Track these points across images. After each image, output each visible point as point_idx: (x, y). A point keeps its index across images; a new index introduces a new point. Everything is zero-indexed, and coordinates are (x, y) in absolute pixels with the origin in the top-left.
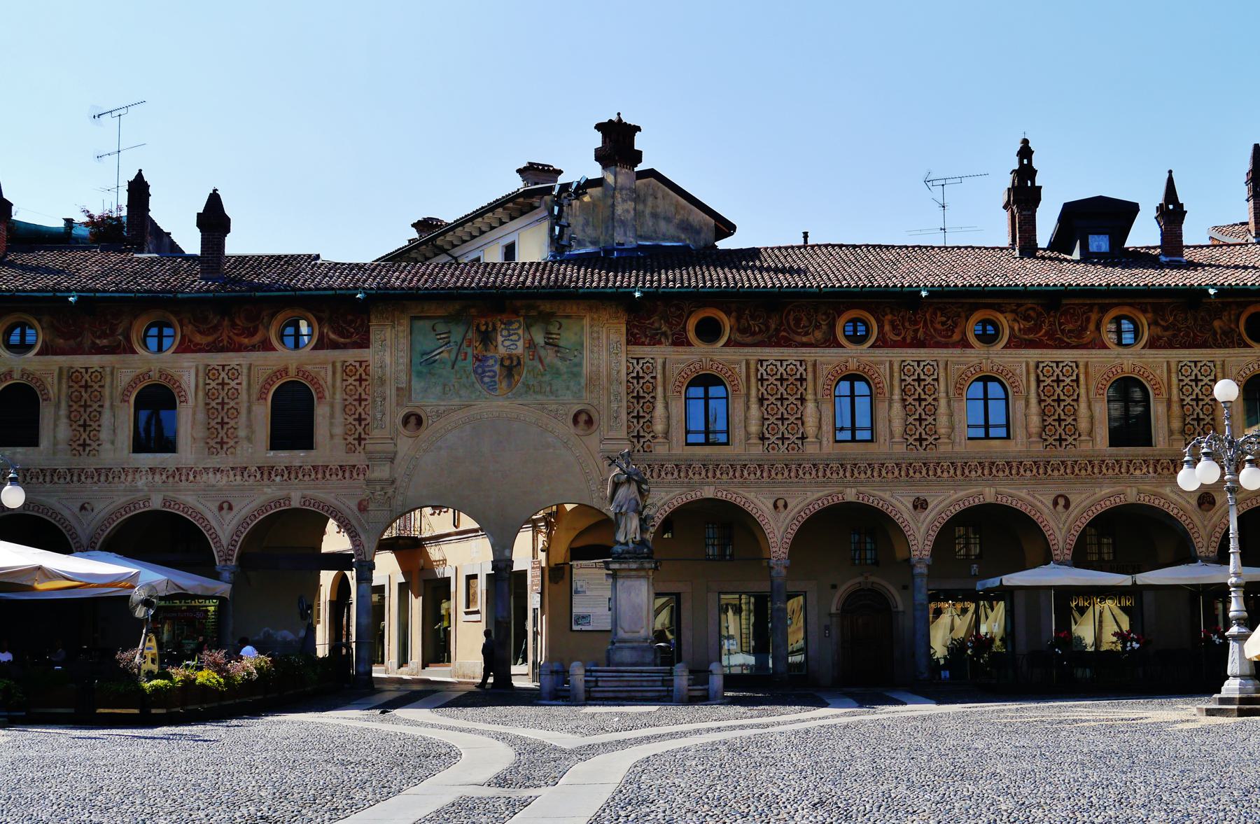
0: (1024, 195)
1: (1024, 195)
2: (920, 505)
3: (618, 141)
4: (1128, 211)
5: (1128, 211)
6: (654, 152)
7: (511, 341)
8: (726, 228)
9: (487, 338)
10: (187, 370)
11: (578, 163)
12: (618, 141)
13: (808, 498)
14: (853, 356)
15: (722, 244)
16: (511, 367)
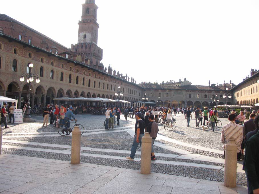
0: (209, 83)
1: (209, 83)
2: (201, 101)
3: (185, 79)
4: (215, 85)
5: (215, 85)
6: (187, 80)
7: (179, 92)
8: (191, 83)
9: (178, 91)
10: (162, 93)
11: (183, 80)
12: (185, 79)
13: (195, 101)
14: (198, 93)
15: (191, 85)
16: (179, 93)
